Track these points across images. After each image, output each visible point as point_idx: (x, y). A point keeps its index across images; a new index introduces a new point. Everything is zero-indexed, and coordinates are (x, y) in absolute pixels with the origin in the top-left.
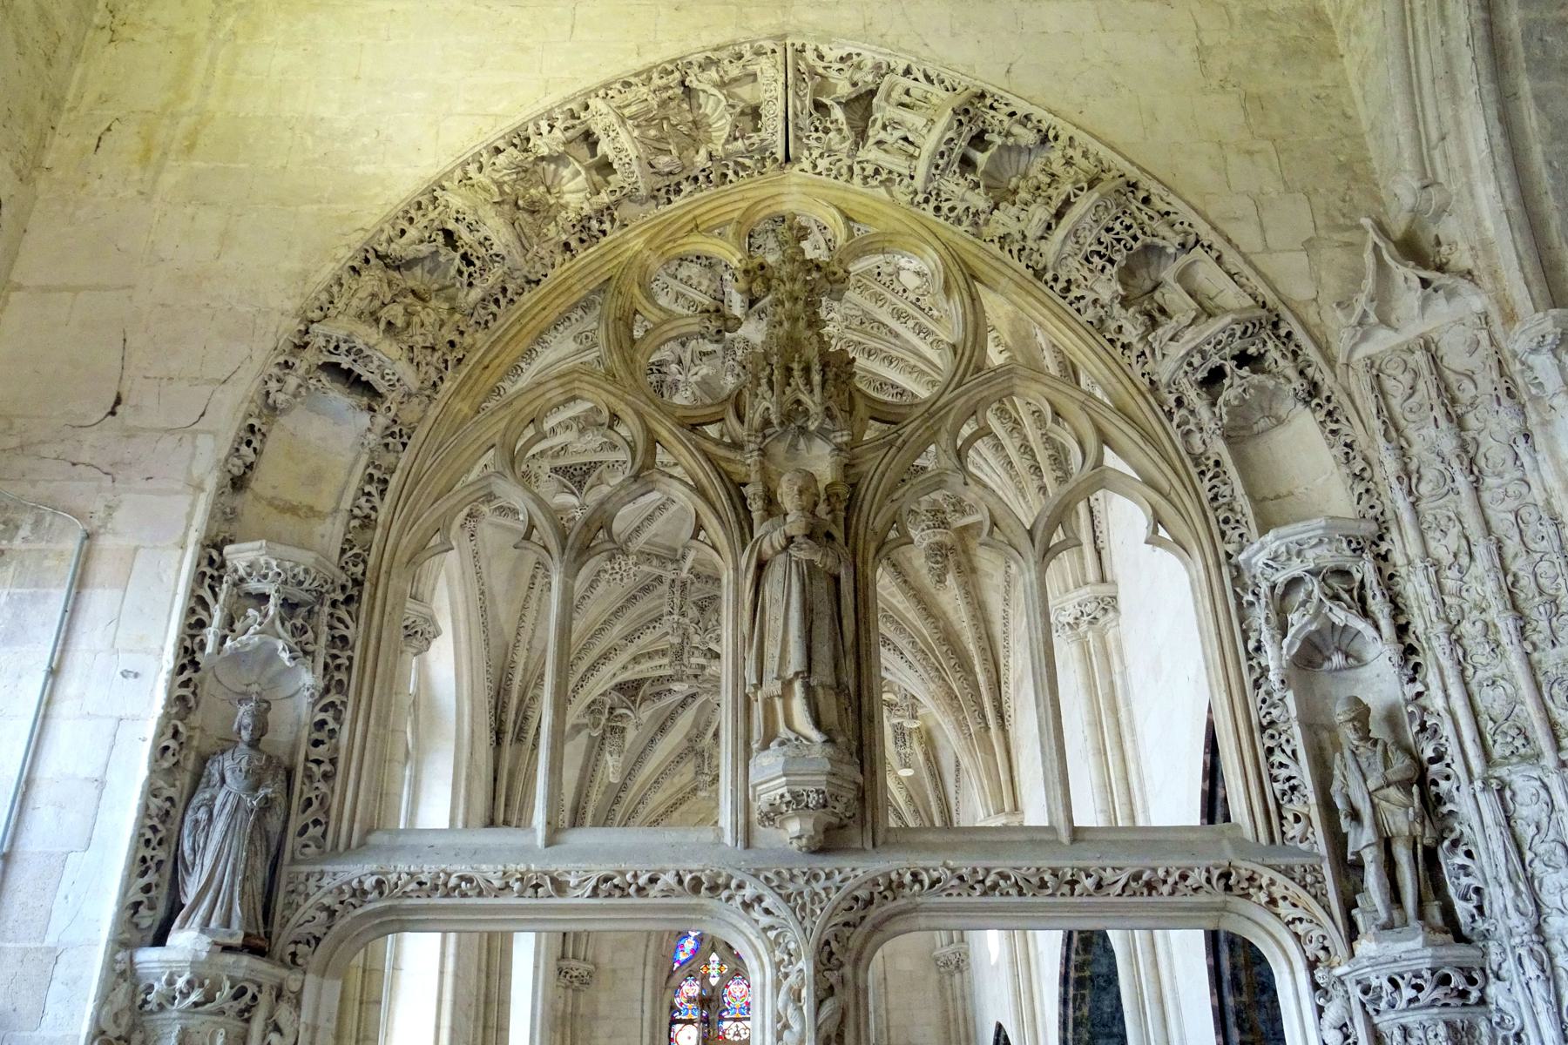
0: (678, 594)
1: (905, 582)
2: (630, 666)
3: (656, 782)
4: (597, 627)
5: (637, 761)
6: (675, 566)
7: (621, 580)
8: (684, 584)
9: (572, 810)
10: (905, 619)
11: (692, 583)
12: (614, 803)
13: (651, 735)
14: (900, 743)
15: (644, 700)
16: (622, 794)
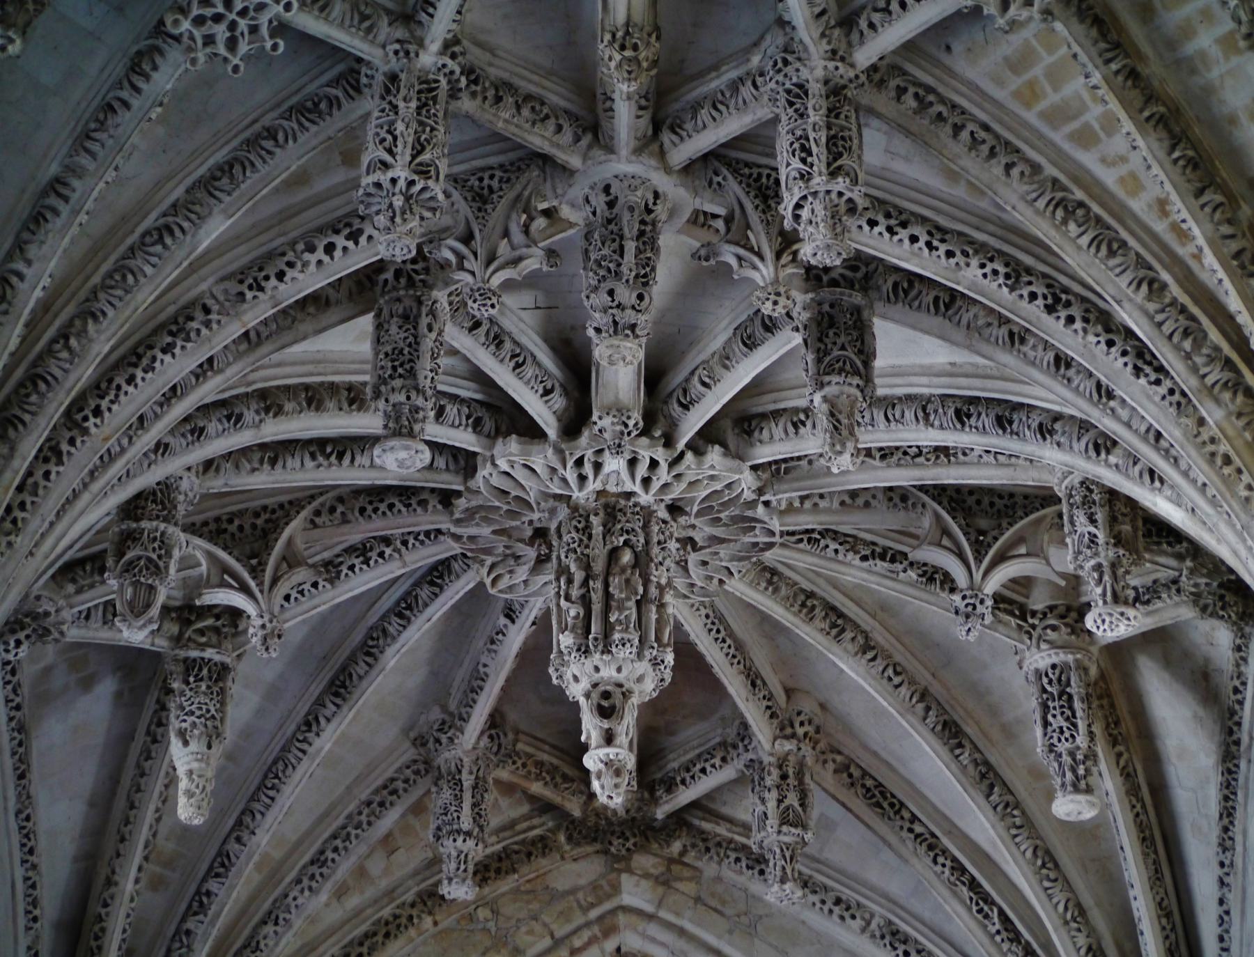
0: (408, 108)
1: (1133, 75)
2: (249, 416)
3: (318, 860)
4: (148, 223)
5: (262, 786)
6: (400, 33)
7: (232, 44)
8: (427, 90)
9: (58, 926)
10: (1122, 213)
11: (454, 93)
12: (189, 912)
13: (303, 708)
14: (1058, 722)
15: (291, 560)
16: (212, 885)
